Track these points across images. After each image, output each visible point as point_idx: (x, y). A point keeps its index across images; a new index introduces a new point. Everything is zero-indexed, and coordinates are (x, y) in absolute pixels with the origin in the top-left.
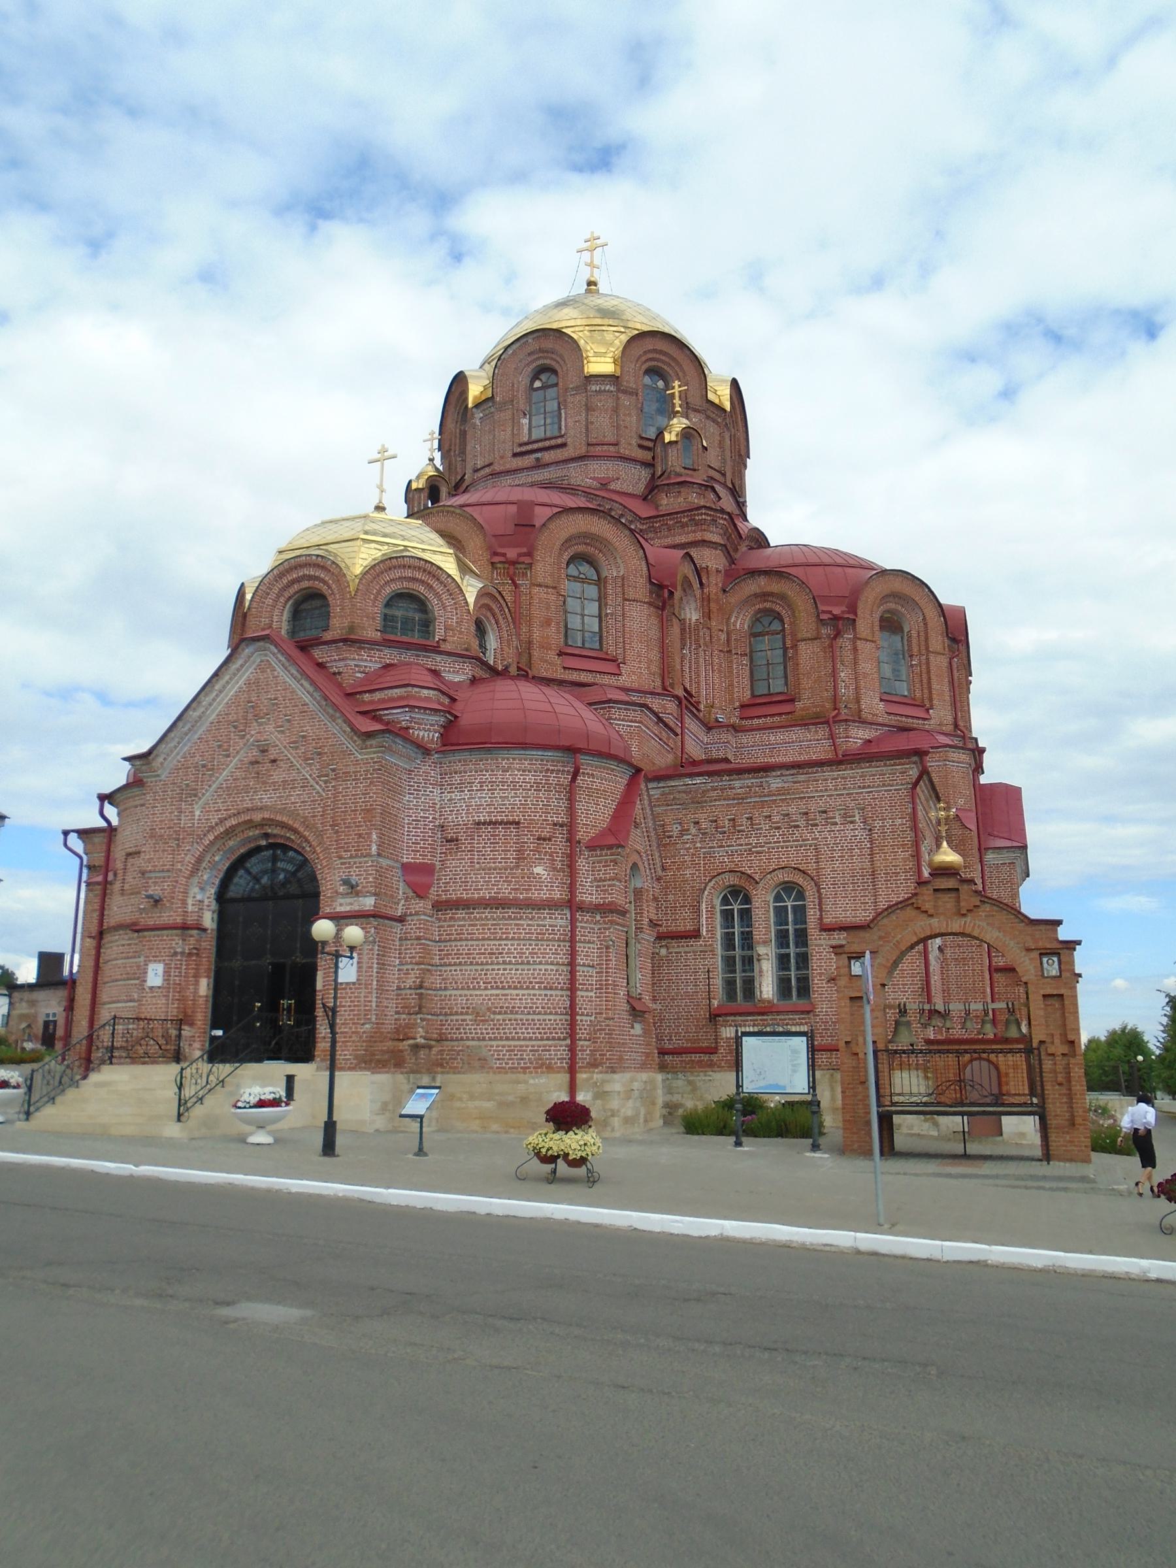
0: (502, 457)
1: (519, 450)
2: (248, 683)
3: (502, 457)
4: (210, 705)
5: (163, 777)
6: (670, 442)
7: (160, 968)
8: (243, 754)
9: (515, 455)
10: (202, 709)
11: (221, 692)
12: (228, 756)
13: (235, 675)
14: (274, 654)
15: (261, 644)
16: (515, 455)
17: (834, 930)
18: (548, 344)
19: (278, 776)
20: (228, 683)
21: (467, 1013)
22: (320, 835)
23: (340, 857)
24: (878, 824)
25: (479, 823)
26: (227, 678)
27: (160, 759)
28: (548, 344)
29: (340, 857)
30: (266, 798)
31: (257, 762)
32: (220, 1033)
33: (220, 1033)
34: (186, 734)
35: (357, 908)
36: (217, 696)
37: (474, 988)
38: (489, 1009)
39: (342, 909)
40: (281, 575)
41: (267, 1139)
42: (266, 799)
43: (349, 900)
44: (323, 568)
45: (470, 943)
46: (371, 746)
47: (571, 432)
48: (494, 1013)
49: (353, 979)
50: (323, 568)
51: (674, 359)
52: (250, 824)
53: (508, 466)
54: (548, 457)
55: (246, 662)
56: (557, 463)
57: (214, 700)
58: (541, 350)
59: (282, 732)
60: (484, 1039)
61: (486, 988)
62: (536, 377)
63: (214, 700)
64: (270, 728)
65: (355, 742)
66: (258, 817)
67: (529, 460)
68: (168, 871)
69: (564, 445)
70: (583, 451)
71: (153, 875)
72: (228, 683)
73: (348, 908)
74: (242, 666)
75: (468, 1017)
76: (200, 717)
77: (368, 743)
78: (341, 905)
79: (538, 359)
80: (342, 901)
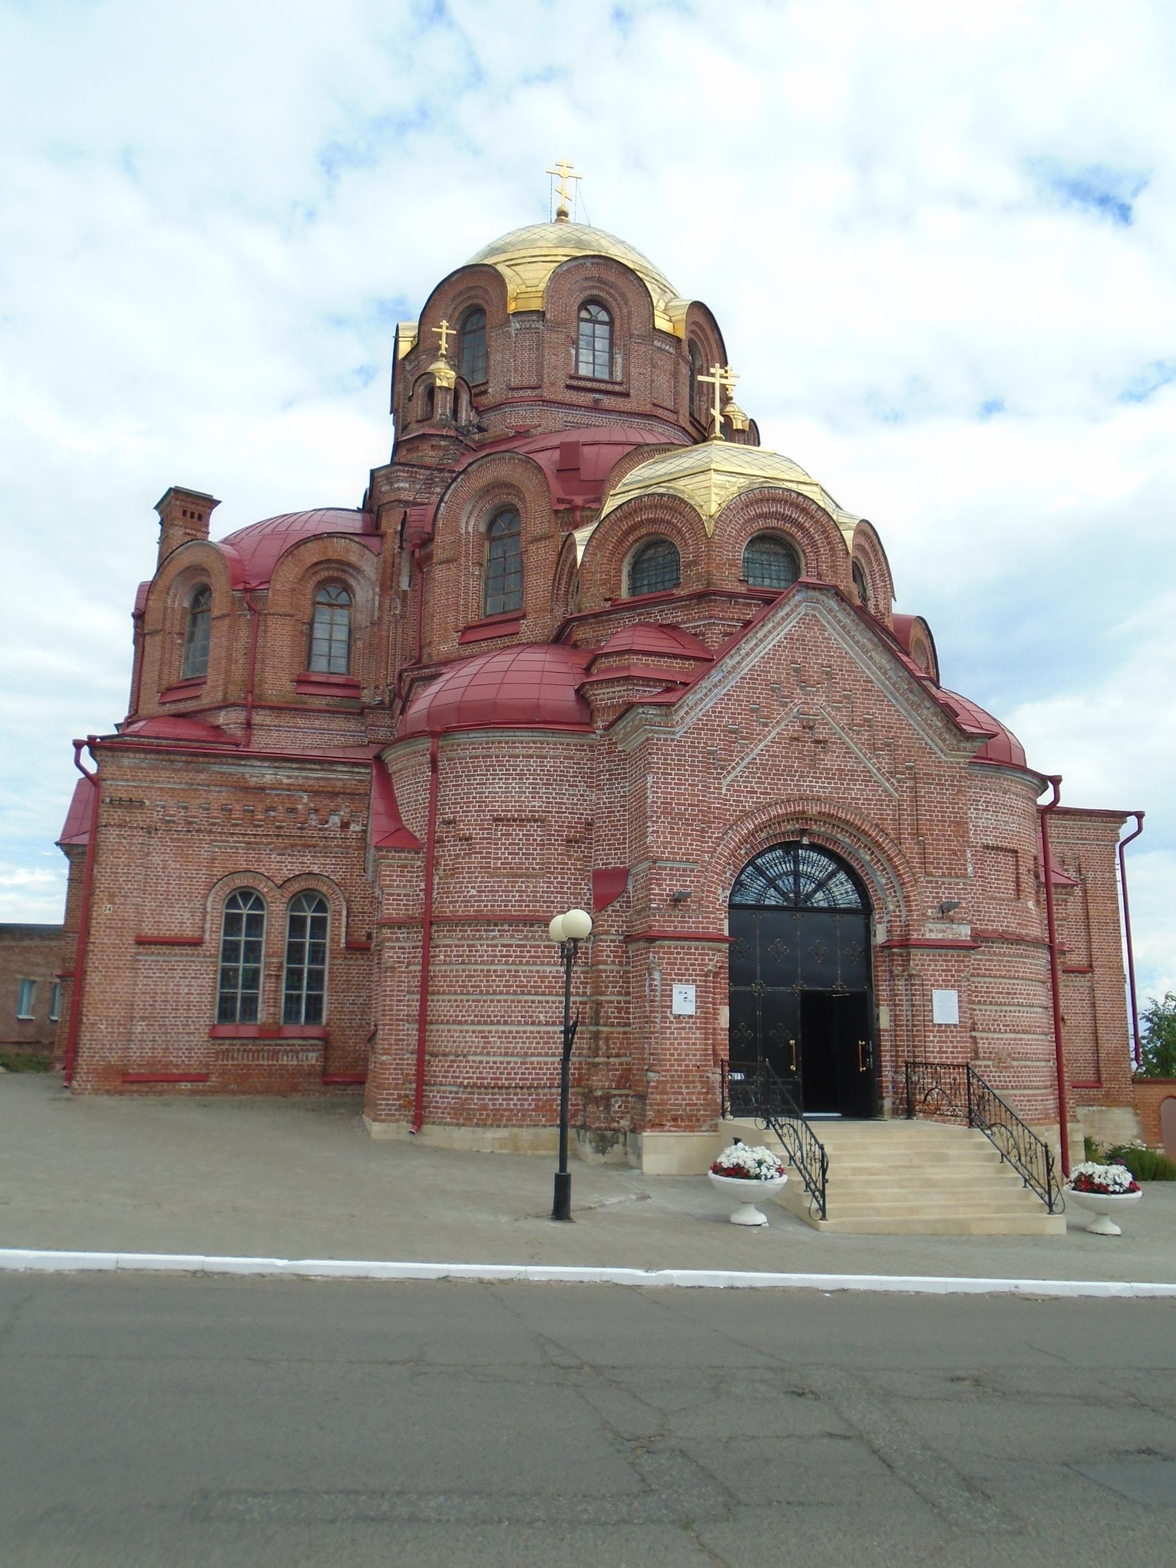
0: (552, 384)
1: (569, 382)
2: (789, 637)
3: (552, 384)
4: (748, 654)
5: (677, 737)
6: (737, 430)
7: (691, 990)
8: (781, 727)
9: (568, 387)
10: (738, 658)
11: (761, 641)
12: (766, 725)
13: (779, 624)
14: (830, 611)
15: (816, 594)
16: (568, 387)
17: (1072, 972)
18: (610, 276)
19: (830, 761)
20: (770, 632)
21: (989, 1059)
22: (899, 841)
23: (928, 874)
24: (1090, 875)
25: (987, 847)
26: (771, 625)
27: (682, 713)
28: (610, 276)
29: (928, 874)
30: (819, 787)
31: (797, 739)
32: (738, 1076)
33: (738, 1076)
34: (715, 686)
35: (950, 937)
36: (756, 645)
37: (995, 1031)
38: (1009, 1055)
39: (933, 936)
40: (748, 505)
41: (1116, 1230)
42: (818, 789)
43: (943, 927)
44: (804, 511)
45: (986, 980)
46: (965, 749)
47: (635, 384)
48: (1014, 1059)
49: (954, 1019)
50: (804, 511)
51: (707, 338)
52: (801, 816)
53: (559, 398)
54: (607, 401)
55: (792, 611)
56: (621, 413)
57: (752, 650)
58: (600, 280)
59: (838, 709)
60: (1007, 1088)
61: (1005, 1032)
62: (583, 306)
63: (752, 650)
64: (822, 700)
65: (944, 740)
66: (813, 809)
67: (586, 398)
68: (695, 862)
69: (626, 395)
70: (648, 408)
71: (669, 865)
72: (770, 632)
73: (940, 936)
74: (788, 615)
75: (990, 1063)
76: (734, 668)
77: (962, 745)
78: (931, 931)
79: (592, 287)
80: (931, 926)
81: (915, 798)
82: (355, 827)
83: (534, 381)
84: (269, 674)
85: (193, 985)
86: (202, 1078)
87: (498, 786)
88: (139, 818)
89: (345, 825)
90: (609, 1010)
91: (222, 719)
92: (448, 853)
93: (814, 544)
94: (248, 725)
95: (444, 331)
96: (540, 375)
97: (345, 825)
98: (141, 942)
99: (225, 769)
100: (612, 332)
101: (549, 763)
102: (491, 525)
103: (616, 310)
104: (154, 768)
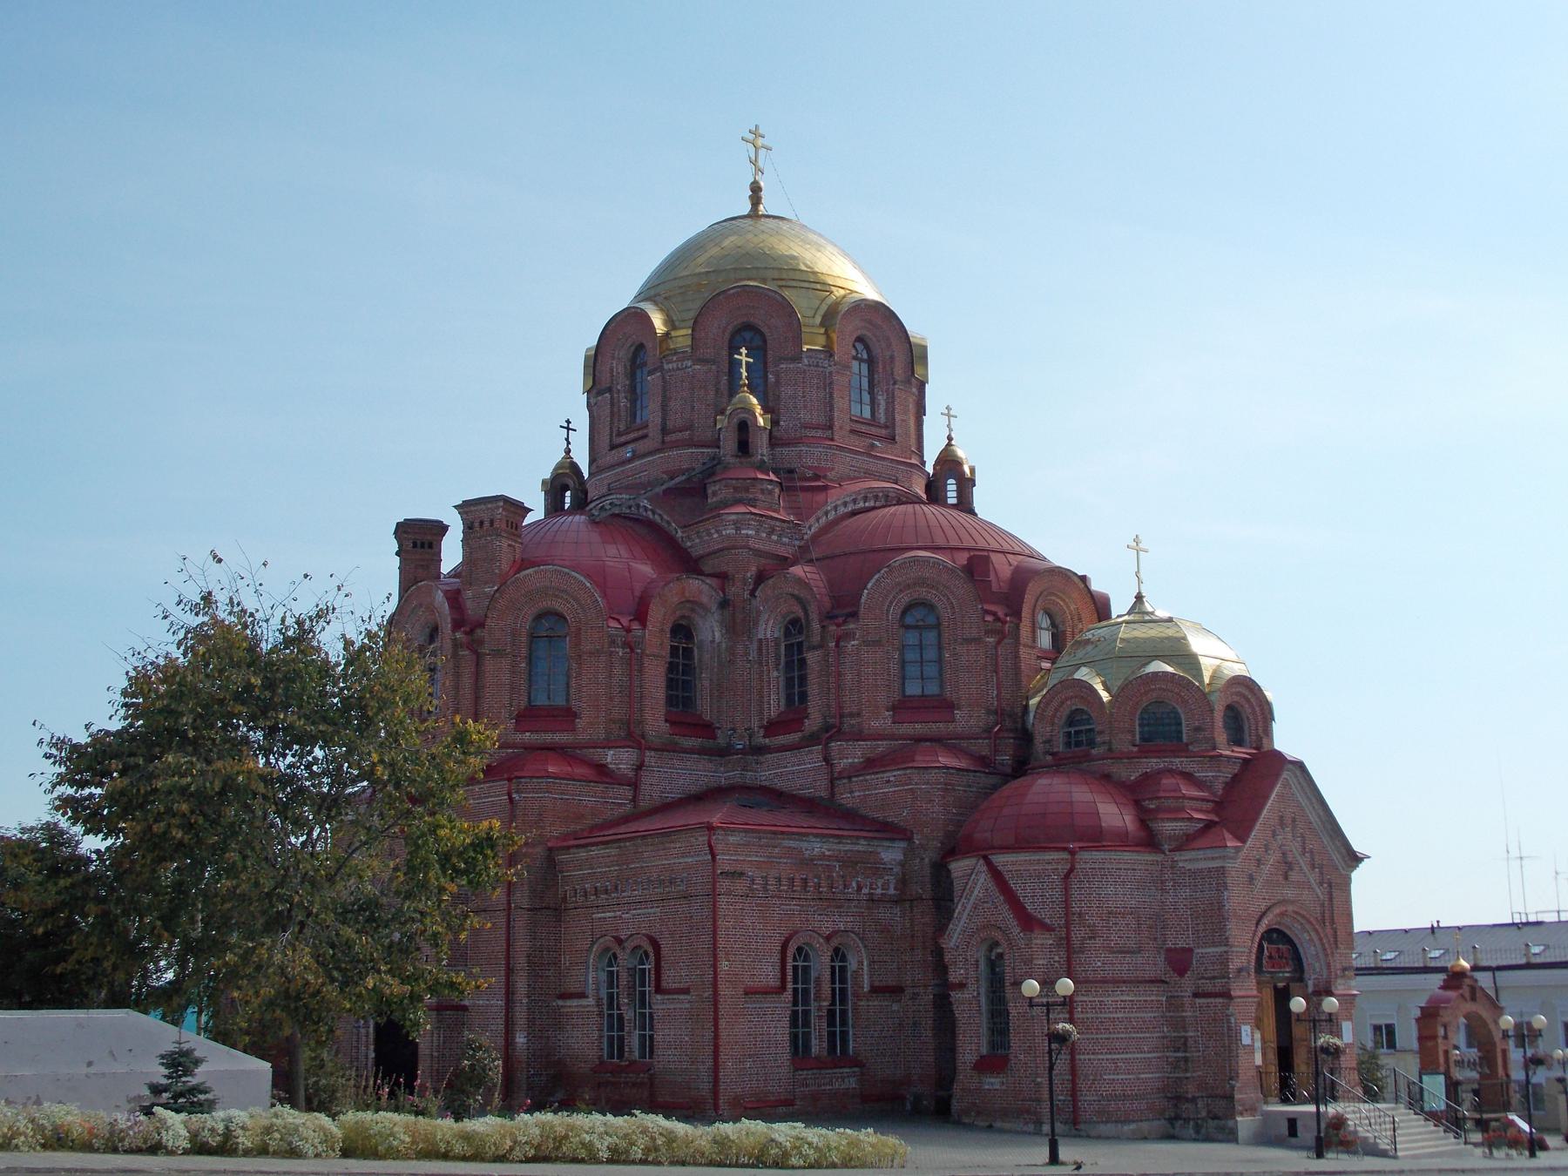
9: (853, 431)
16: (853, 431)
30: (1289, 893)
58: (870, 322)
64: (1290, 836)
81: (1331, 899)
82: (865, 891)
83: (822, 420)
84: (648, 716)
85: (775, 1022)
86: (789, 1103)
87: (1111, 890)
88: (740, 886)
89: (859, 888)
90: (1191, 1042)
91: (610, 757)
92: (1078, 934)
93: (1254, 713)
94: (640, 767)
95: (744, 359)
96: (831, 419)
97: (859, 888)
98: (749, 992)
99: (792, 844)
100: (871, 372)
101: (1138, 873)
102: (904, 613)
103: (876, 351)
104: (747, 845)
